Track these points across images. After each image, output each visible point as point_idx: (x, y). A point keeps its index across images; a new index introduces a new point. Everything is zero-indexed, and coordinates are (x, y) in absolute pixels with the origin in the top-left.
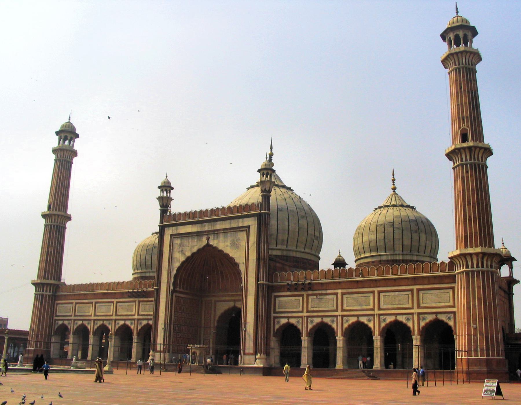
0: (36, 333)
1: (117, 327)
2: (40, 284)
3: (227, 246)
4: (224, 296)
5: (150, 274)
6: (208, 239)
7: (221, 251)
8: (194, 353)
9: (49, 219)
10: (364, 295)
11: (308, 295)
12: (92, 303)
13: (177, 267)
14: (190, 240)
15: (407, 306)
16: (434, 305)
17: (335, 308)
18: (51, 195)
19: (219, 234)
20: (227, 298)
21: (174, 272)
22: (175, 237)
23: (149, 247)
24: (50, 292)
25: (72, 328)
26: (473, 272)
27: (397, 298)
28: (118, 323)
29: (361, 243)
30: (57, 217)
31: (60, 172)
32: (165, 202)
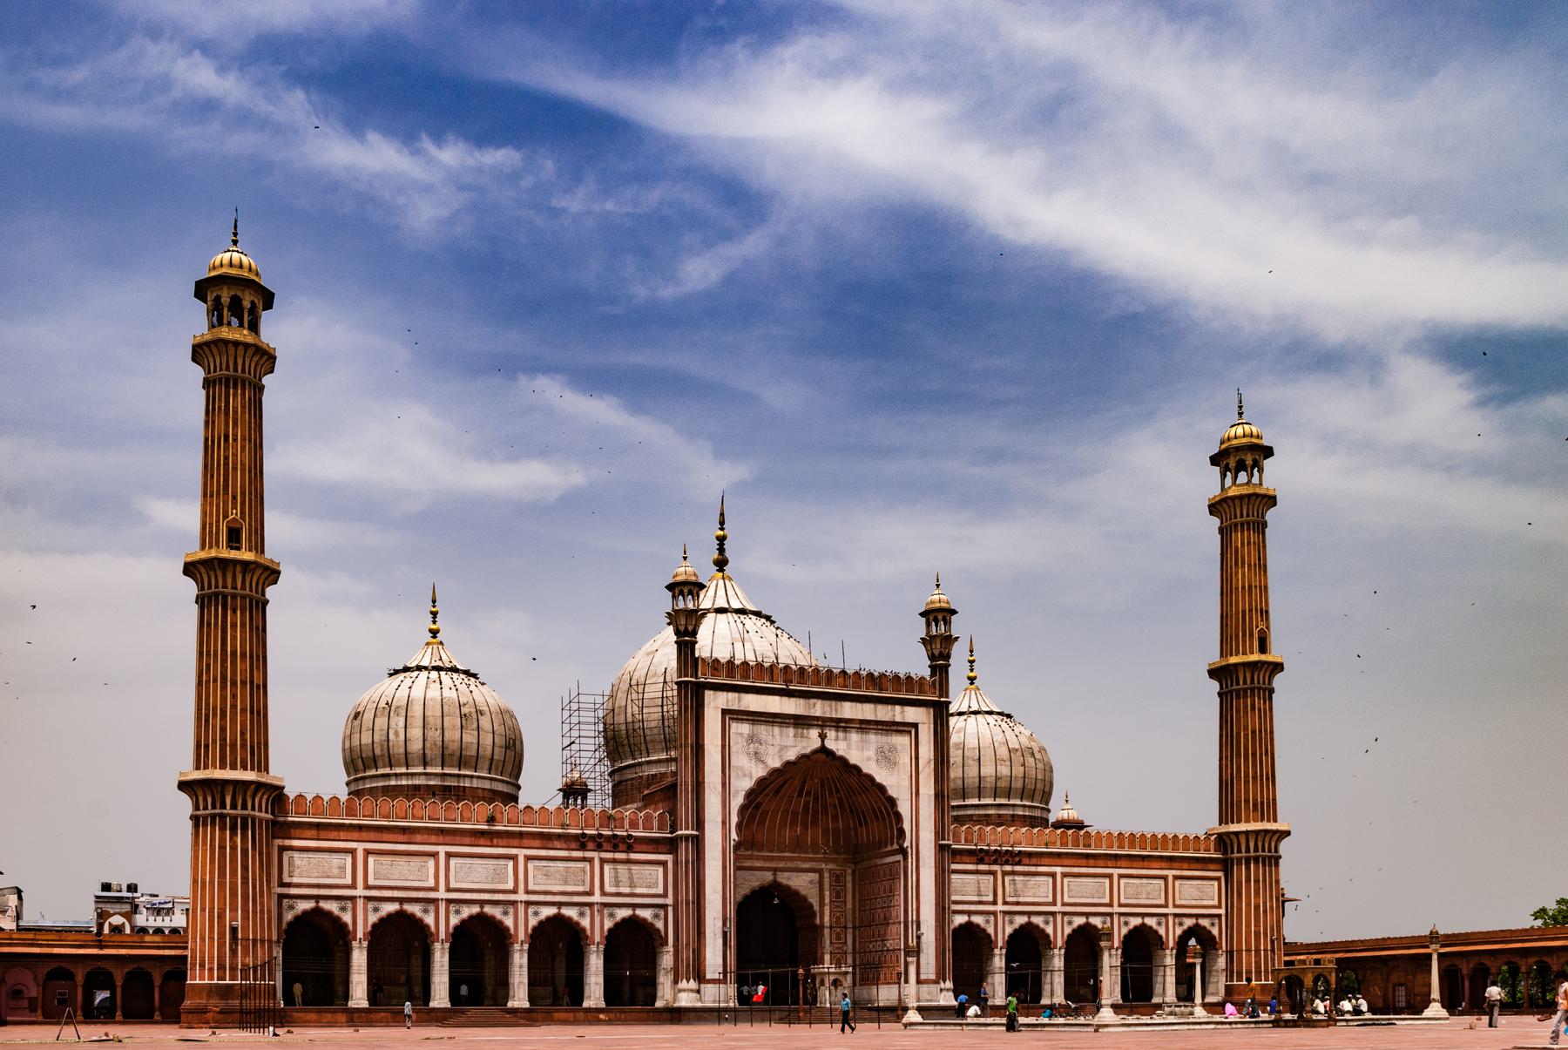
0: (251, 938)
1: (533, 922)
3: (869, 759)
4: (750, 858)
5: (471, 783)
6: (823, 737)
7: (857, 769)
10: (1097, 880)
11: (1005, 873)
12: (435, 855)
14: (777, 729)
17: (1050, 899)
20: (758, 864)
21: (737, 801)
22: (735, 717)
23: (465, 710)
25: (361, 921)
26: (1270, 858)
27: (1144, 889)
28: (536, 914)
29: (973, 778)
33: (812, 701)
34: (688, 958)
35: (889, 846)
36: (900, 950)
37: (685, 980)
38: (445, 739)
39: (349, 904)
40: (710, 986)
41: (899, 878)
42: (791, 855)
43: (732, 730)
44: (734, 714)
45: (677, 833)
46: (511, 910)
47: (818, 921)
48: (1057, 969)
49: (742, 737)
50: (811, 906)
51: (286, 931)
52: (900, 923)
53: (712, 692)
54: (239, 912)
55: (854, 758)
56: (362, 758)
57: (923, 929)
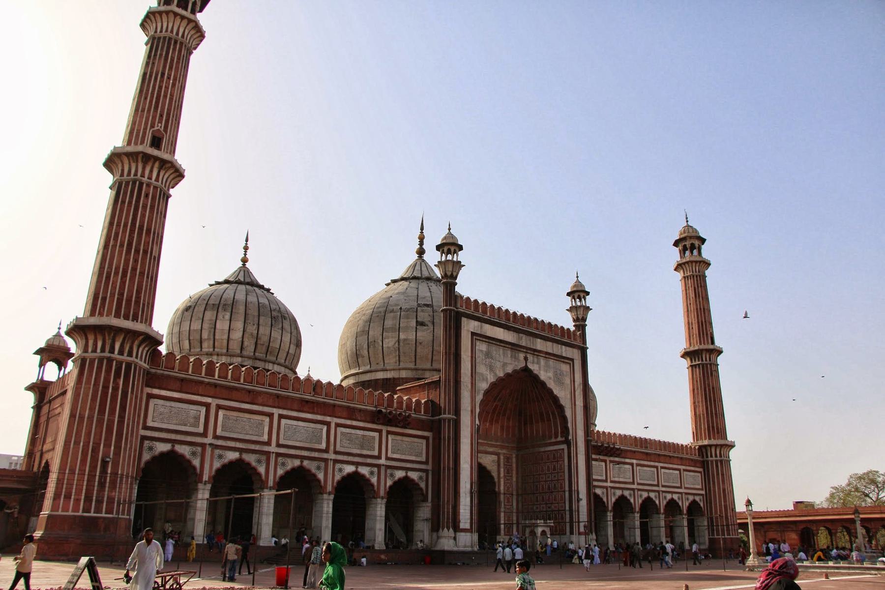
1: (338, 477)
2: (141, 338)
6: (526, 359)
7: (543, 384)
8: (543, 532)
9: (158, 175)
12: (271, 415)
13: (485, 389)
15: (678, 485)
16: (692, 486)
18: (161, 116)
19: (539, 357)
21: (479, 397)
22: (479, 338)
23: (274, 314)
24: (145, 362)
28: (340, 470)
30: (172, 177)
31: (182, 74)
32: (450, 268)
33: (521, 335)
34: (448, 512)
35: (553, 438)
36: (565, 510)
37: (446, 528)
38: (260, 333)
39: (199, 449)
40: (463, 534)
41: (564, 461)
42: (483, 441)
43: (477, 348)
44: (478, 336)
45: (441, 416)
46: (323, 464)
47: (497, 490)
48: (655, 526)
49: (482, 353)
50: (492, 477)
51: (144, 470)
52: (564, 491)
53: (466, 319)
54: (112, 448)
55: (543, 376)
56: (189, 340)
57: (581, 496)
